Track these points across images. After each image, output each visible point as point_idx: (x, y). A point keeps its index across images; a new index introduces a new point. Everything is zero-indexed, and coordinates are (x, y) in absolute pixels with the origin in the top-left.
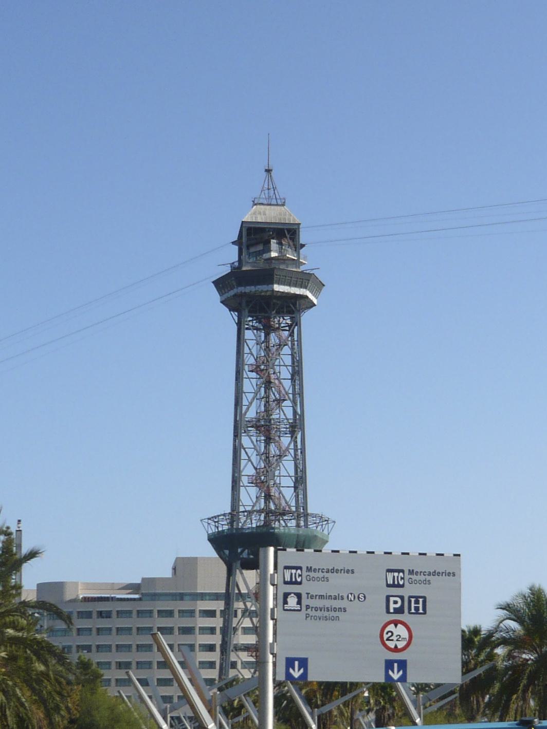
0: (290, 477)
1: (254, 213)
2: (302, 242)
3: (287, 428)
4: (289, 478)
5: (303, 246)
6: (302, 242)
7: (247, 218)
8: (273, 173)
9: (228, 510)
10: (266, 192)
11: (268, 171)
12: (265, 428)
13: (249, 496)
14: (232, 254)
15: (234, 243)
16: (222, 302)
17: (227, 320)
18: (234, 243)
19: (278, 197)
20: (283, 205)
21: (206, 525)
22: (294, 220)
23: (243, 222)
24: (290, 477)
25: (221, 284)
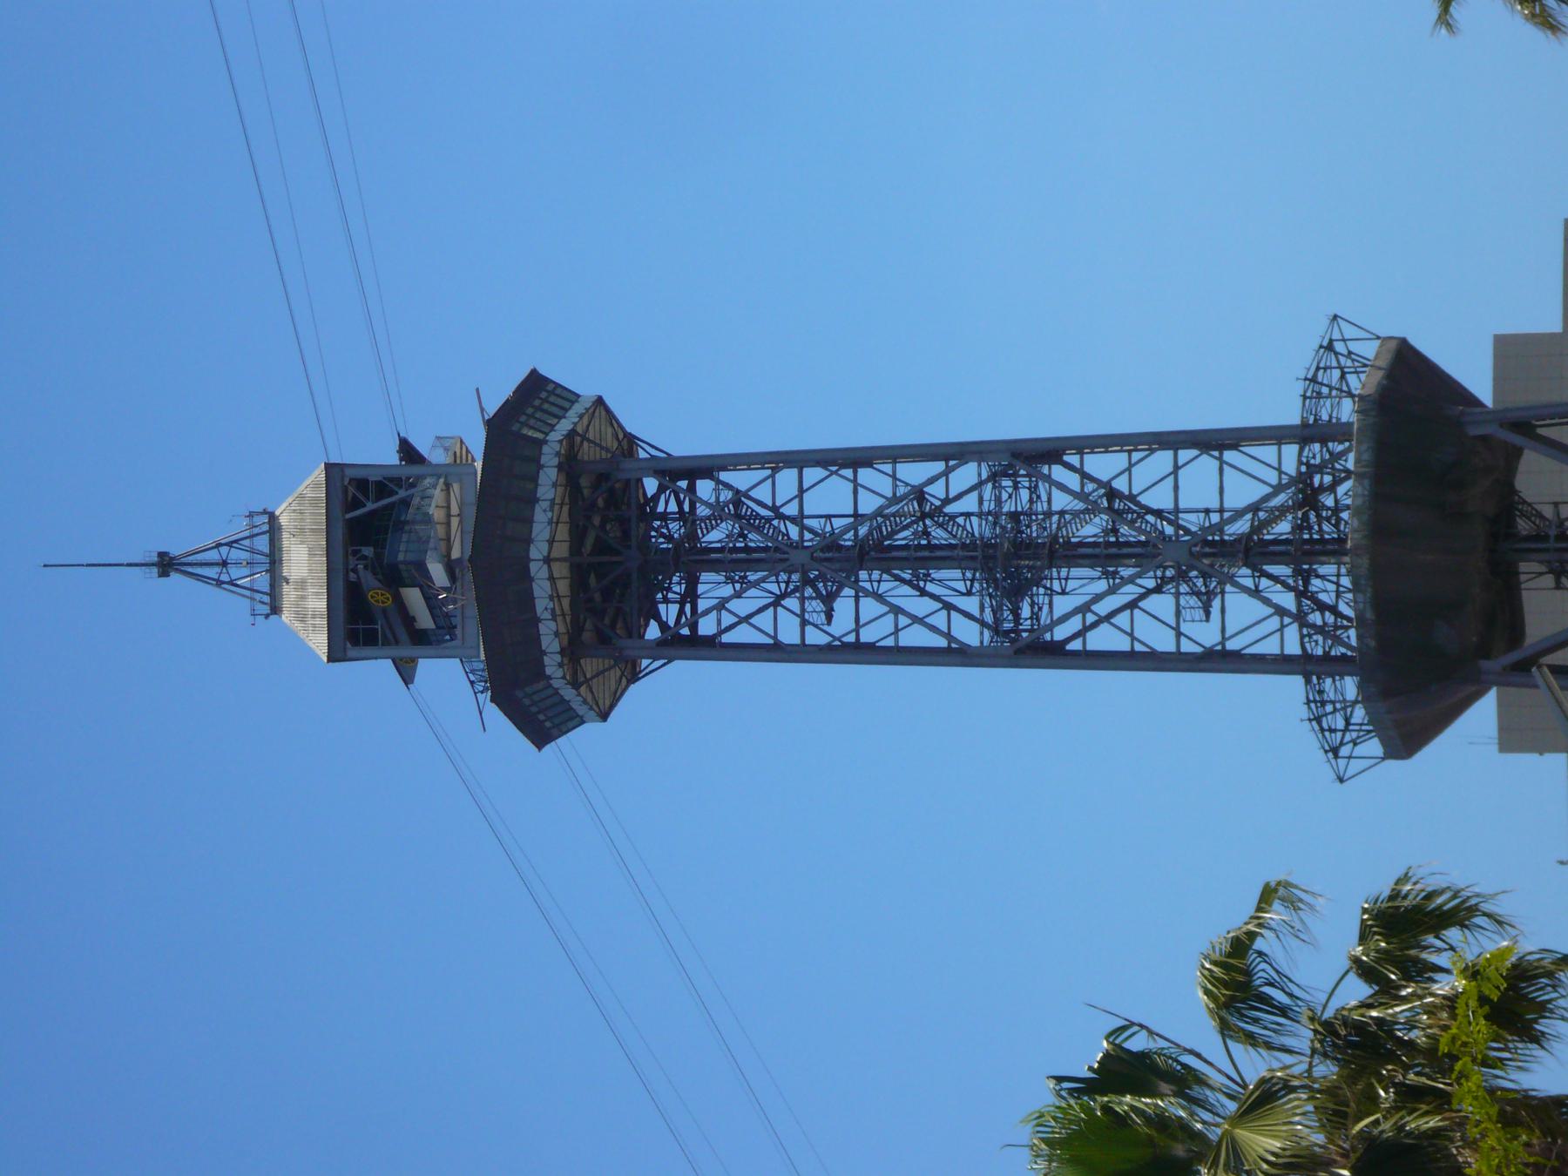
0: (1177, 468)
1: (302, 618)
2: (390, 456)
3: (1016, 487)
4: (1181, 472)
5: (408, 452)
6: (390, 456)
7: (318, 642)
8: (175, 551)
9: (1293, 685)
10: (235, 572)
11: (166, 564)
12: (1013, 562)
13: (1248, 614)
14: (447, 679)
15: (408, 679)
16: (604, 716)
17: (668, 698)
18: (408, 679)
19: (247, 533)
20: (273, 518)
21: (1355, 766)
22: (316, 485)
23: (330, 659)
24: (1177, 468)
25: (541, 723)
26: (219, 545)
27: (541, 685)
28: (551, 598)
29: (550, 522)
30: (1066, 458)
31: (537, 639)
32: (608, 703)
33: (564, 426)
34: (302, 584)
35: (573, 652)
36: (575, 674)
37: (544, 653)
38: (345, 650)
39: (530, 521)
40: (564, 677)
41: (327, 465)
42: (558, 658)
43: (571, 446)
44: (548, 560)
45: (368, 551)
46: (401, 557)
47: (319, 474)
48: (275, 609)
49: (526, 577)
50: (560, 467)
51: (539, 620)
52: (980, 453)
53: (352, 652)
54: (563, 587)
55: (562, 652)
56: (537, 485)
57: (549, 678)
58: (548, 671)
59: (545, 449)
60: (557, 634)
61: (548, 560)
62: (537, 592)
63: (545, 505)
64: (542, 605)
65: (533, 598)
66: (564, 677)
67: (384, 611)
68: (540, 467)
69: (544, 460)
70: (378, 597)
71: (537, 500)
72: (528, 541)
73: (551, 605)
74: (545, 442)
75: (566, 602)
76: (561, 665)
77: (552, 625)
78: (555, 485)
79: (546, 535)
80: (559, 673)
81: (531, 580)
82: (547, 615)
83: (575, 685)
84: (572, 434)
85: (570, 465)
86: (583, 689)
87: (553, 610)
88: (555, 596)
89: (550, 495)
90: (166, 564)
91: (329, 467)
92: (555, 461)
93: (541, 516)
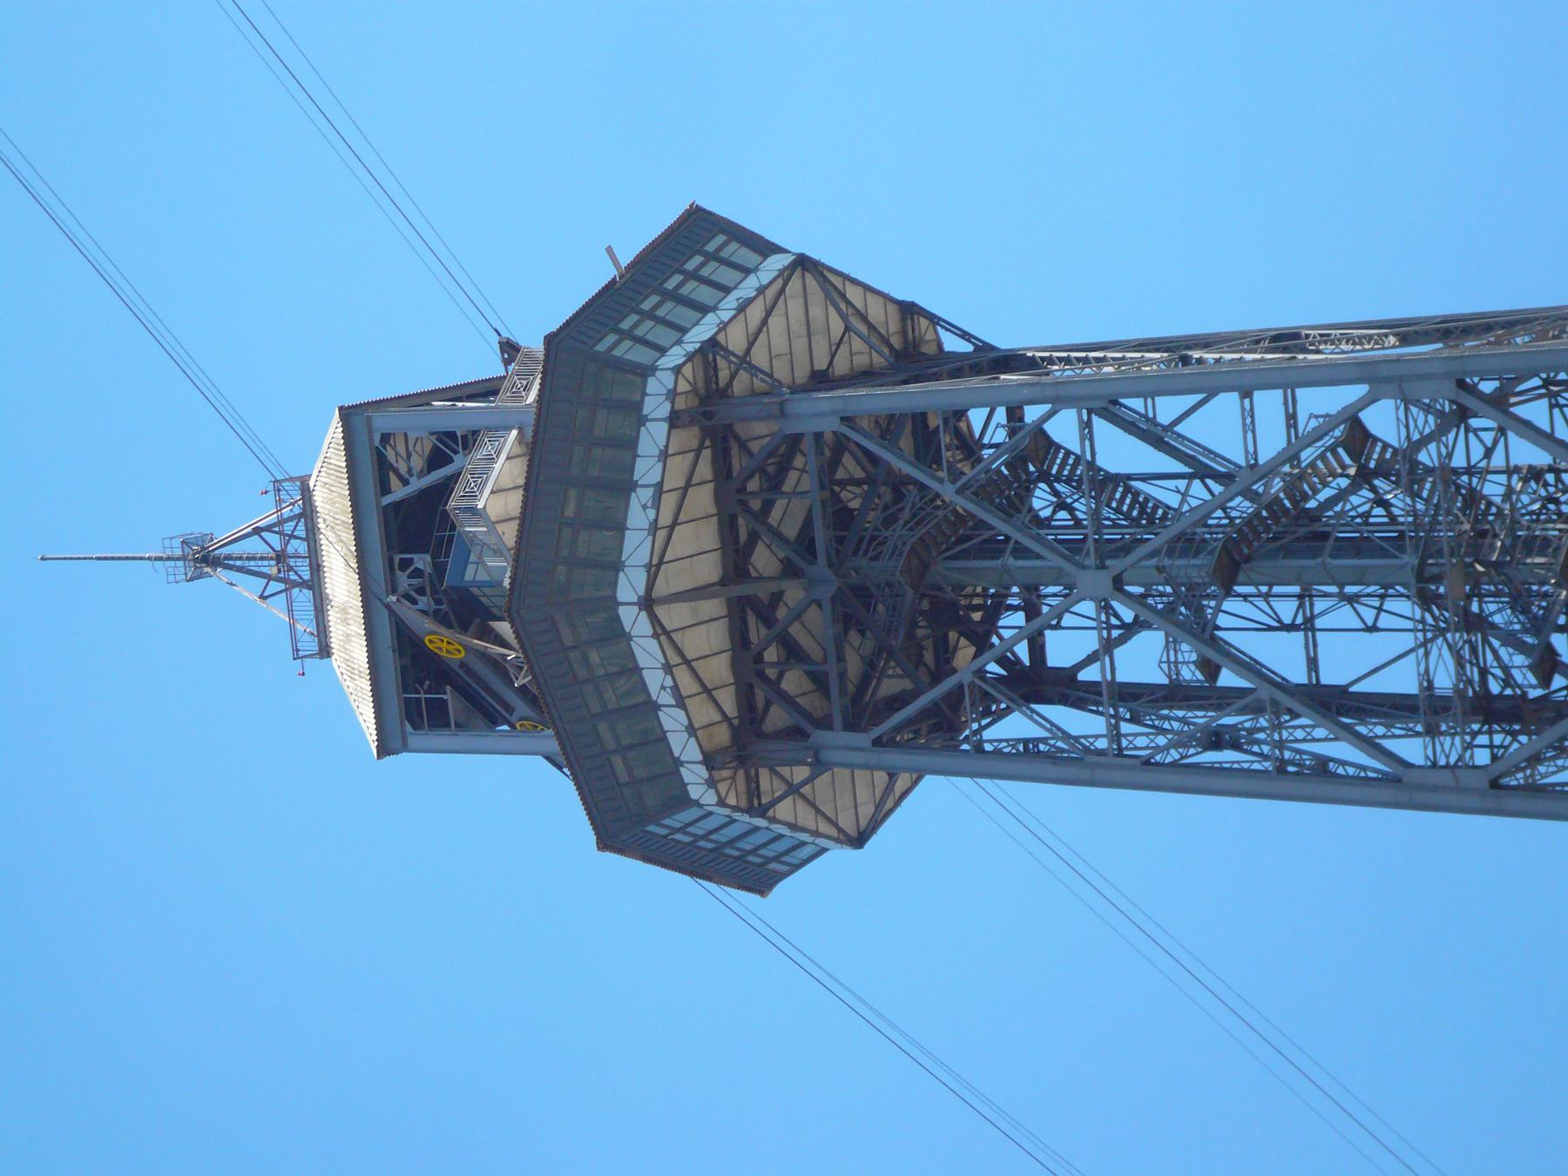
11: (204, 558)
23: (384, 750)
26: (257, 531)
27: (689, 815)
28: (668, 668)
29: (654, 528)
30: (1376, 482)
31: (662, 738)
32: (866, 811)
33: (702, 331)
34: (344, 611)
35: (745, 745)
36: (753, 791)
37: (678, 763)
38: (404, 738)
39: (620, 528)
40: (722, 803)
41: (341, 409)
42: (703, 771)
43: (711, 369)
44: (648, 603)
45: (422, 561)
46: (469, 576)
47: (335, 431)
48: (325, 651)
49: (617, 635)
50: (674, 421)
51: (656, 707)
52: (1399, 380)
53: (413, 740)
54: (708, 637)
55: (709, 760)
56: (635, 456)
57: (697, 803)
58: (695, 792)
59: (652, 385)
60: (691, 730)
61: (648, 603)
62: (642, 659)
63: (644, 495)
64: (655, 680)
65: (637, 670)
66: (722, 803)
67: (462, 664)
68: (642, 420)
69: (649, 406)
70: (446, 644)
71: (632, 486)
72: (617, 566)
73: (669, 682)
74: (651, 370)
75: (719, 670)
76: (711, 783)
77: (680, 714)
78: (664, 455)
79: (643, 555)
80: (710, 798)
81: (627, 637)
82: (666, 698)
83: (759, 809)
84: (713, 343)
85: (710, 412)
86: (784, 810)
87: (675, 689)
88: (679, 660)
89: (654, 477)
90: (204, 558)
91: (347, 414)
92: (665, 410)
93: (638, 516)
